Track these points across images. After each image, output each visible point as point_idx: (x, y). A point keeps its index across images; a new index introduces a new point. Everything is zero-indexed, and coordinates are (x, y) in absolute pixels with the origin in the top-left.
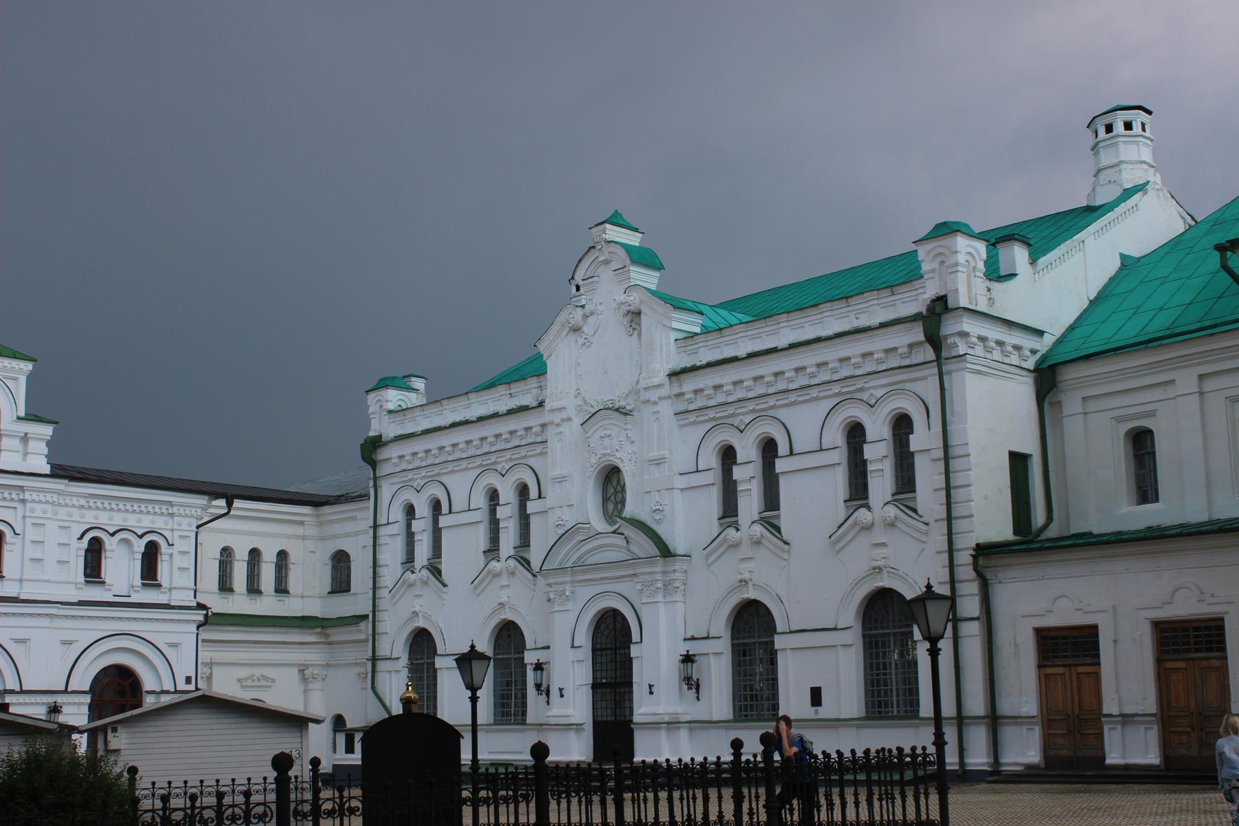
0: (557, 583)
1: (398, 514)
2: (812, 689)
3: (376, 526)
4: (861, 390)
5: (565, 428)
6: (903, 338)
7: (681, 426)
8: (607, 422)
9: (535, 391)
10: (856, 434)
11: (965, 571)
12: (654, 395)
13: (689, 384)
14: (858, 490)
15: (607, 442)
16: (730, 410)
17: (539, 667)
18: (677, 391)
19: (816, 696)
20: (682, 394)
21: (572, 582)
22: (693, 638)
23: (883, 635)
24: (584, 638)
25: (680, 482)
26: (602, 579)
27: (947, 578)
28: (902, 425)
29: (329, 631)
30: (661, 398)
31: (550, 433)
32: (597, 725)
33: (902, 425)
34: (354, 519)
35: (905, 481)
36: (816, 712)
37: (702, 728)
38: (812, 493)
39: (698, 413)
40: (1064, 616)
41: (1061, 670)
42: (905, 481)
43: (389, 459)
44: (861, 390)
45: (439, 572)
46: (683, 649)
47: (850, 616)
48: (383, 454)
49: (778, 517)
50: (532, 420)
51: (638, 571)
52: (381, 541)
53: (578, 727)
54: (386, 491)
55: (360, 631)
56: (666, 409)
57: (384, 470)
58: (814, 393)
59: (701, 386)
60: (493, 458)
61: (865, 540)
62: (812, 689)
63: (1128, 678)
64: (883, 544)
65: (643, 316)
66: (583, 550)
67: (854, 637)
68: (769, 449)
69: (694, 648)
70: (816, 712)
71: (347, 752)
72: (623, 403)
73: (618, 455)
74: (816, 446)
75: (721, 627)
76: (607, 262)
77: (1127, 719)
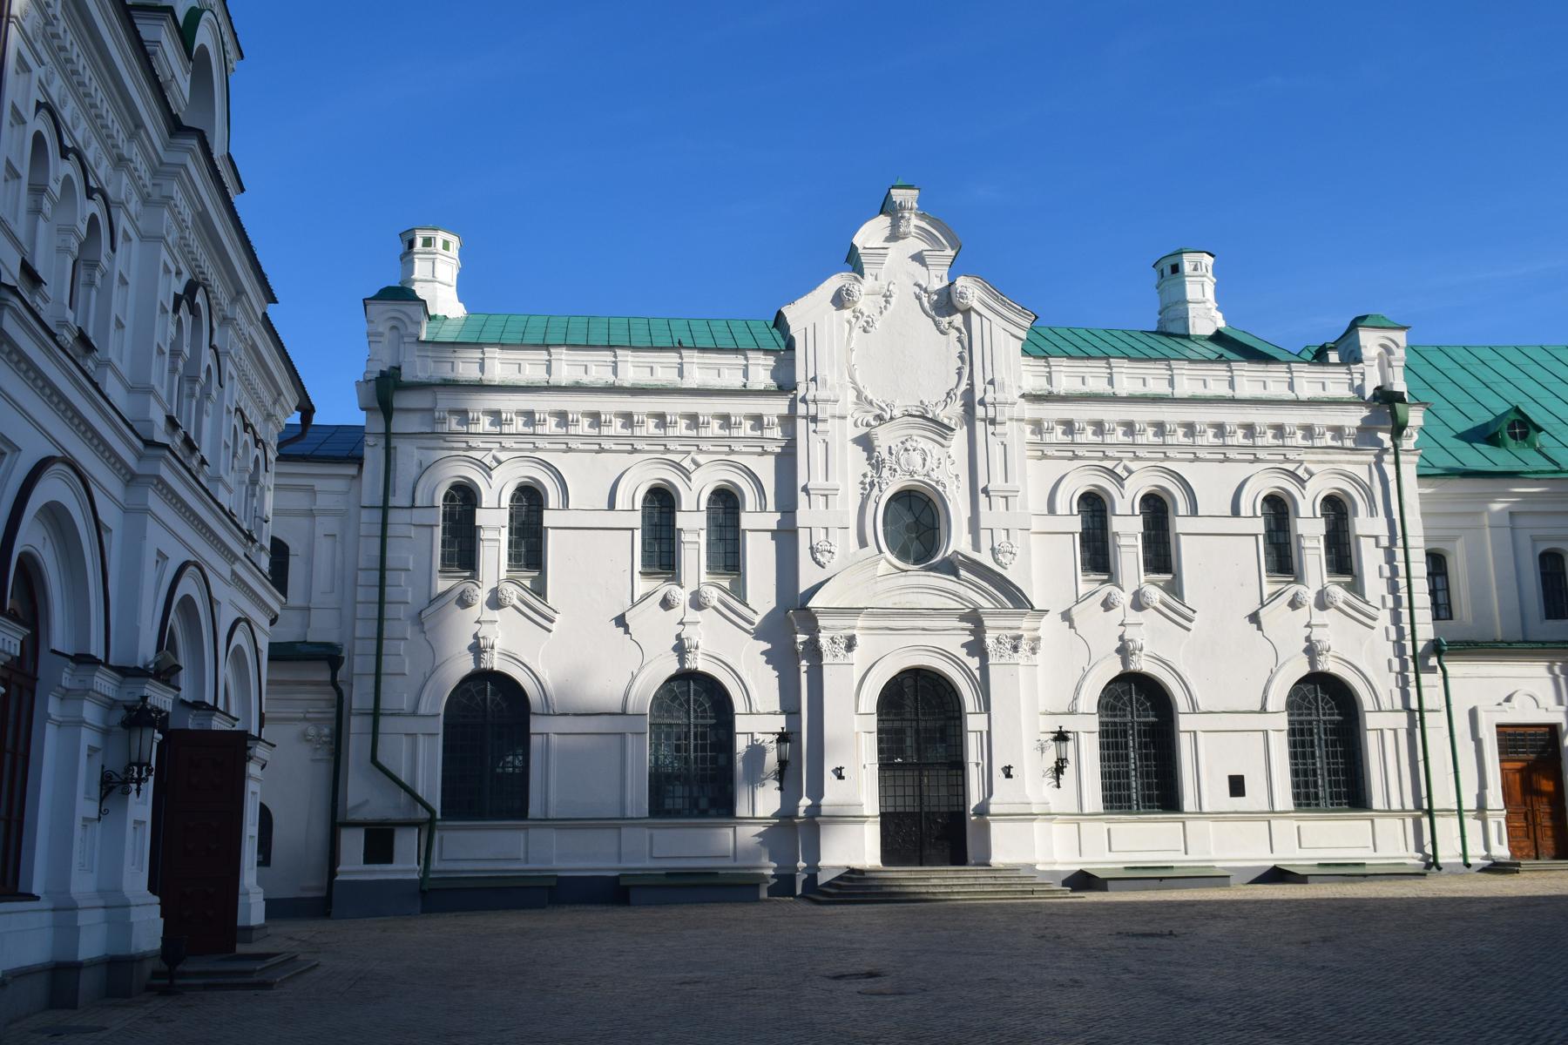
2: (1231, 777)
10: (1278, 509)
19: (1237, 786)
25: (1036, 524)
28: (1336, 509)
32: (882, 815)
47: (1278, 698)
48: (401, 400)
52: (391, 531)
57: (400, 424)
62: (1231, 777)
69: (1068, 724)
71: (369, 859)
73: (934, 475)
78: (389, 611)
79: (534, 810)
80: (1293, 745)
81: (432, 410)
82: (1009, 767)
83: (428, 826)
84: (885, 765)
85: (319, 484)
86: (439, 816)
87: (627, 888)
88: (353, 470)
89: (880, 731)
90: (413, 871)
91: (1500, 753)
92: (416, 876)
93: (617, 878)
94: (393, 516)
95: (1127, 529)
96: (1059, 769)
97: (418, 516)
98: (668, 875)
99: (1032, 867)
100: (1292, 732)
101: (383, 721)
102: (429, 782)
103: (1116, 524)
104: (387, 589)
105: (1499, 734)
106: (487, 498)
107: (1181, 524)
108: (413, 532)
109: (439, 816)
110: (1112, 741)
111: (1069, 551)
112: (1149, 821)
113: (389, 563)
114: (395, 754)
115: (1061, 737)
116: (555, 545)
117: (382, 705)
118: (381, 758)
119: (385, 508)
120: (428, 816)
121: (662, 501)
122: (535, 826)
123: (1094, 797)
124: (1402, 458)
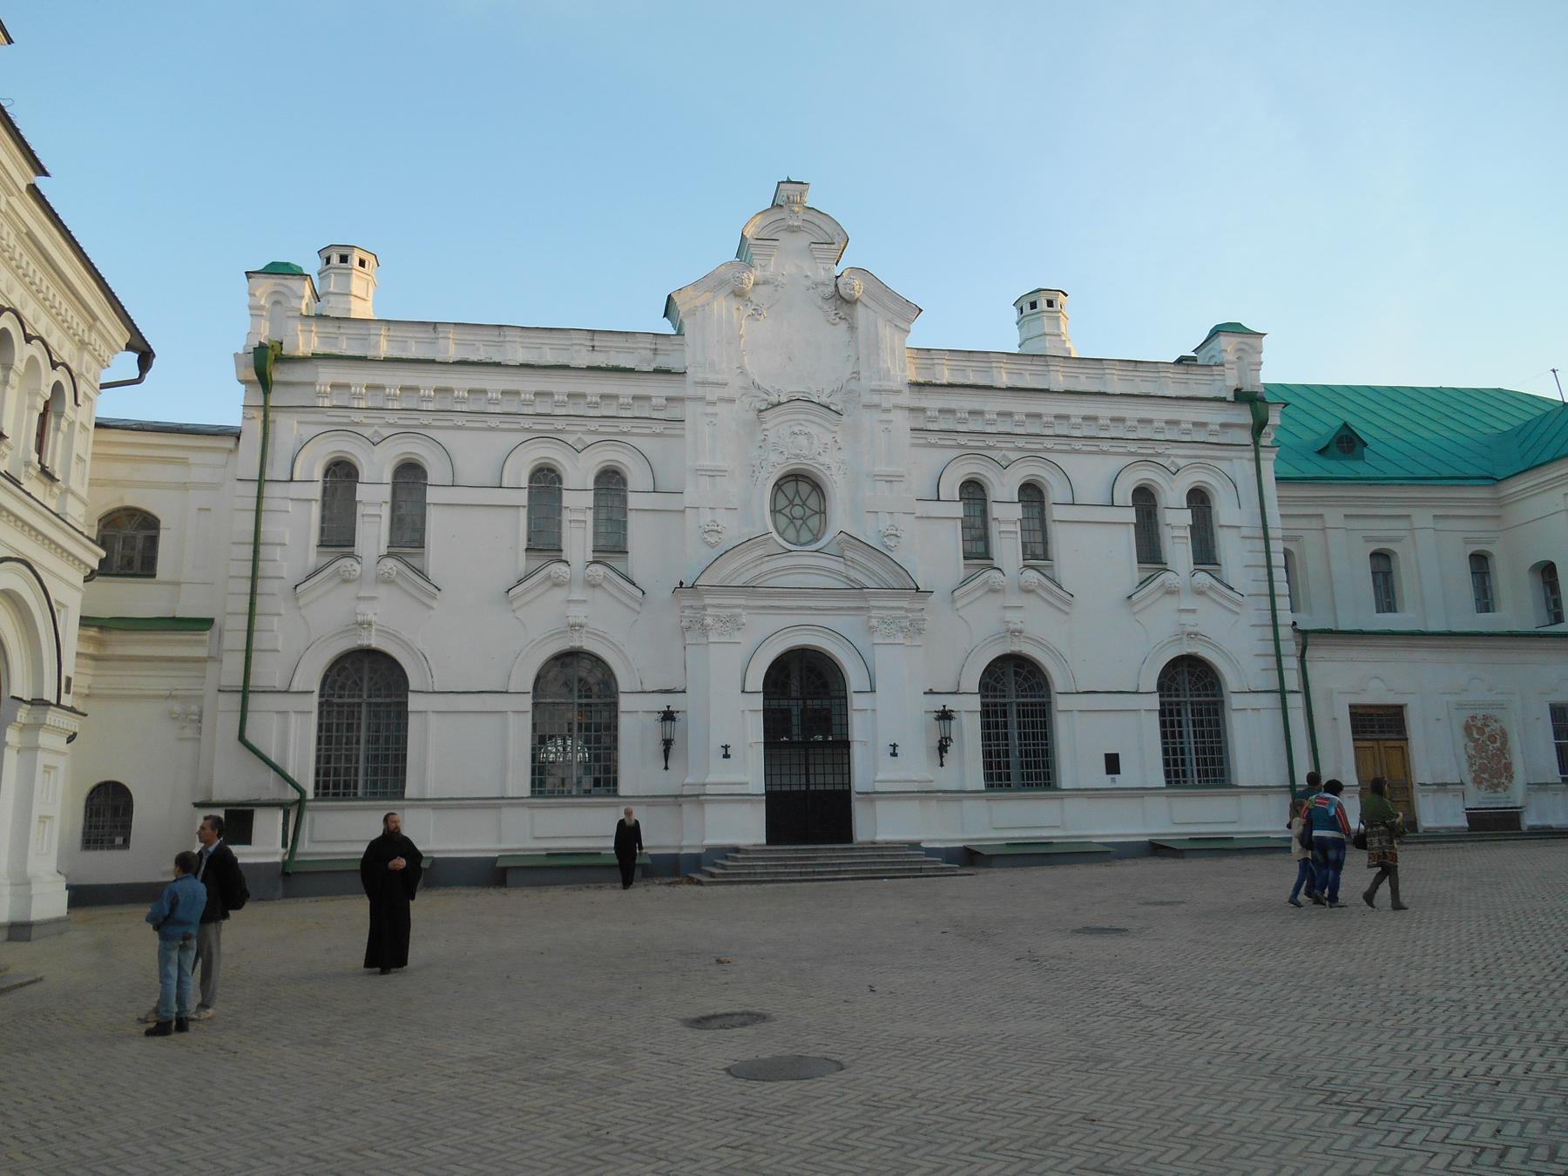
0: (719, 606)
1: (313, 466)
3: (261, 481)
4: (1158, 455)
5: (721, 409)
6: (1214, 416)
7: (914, 445)
8: (802, 416)
9: (649, 354)
10: (1145, 498)
11: (1290, 647)
12: (887, 401)
13: (933, 401)
14: (1150, 551)
15: (803, 440)
16: (991, 441)
17: (668, 716)
18: (916, 404)
19: (1112, 764)
20: (923, 410)
21: (746, 607)
22: (931, 692)
23: (1178, 704)
24: (756, 681)
26: (802, 608)
27: (1272, 651)
28: (1199, 499)
29: (107, 636)
30: (896, 407)
31: (690, 411)
32: (769, 794)
33: (1199, 499)
34: (184, 462)
35: (1205, 553)
36: (1113, 780)
37: (952, 800)
38: (1095, 549)
39: (942, 435)
40: (1377, 694)
41: (1370, 744)
42: (1205, 553)
43: (313, 384)
44: (1158, 455)
45: (421, 573)
46: (938, 703)
49: (1051, 567)
50: (659, 389)
51: (873, 603)
53: (745, 797)
54: (288, 429)
55: (201, 643)
56: (902, 421)
58: (1105, 446)
59: (953, 406)
60: (560, 424)
61: (1170, 603)
63: (1434, 753)
64: (1194, 611)
65: (859, 306)
66: (765, 567)
67: (1154, 702)
68: (1032, 493)
69: (951, 703)
70: (1113, 780)
72: (824, 400)
73: (821, 459)
74: (1106, 499)
75: (972, 681)
76: (792, 230)
77: (1442, 787)
78: (262, 586)
79: (410, 791)
80: (1163, 724)
81: (313, 384)
82: (894, 746)
83: (295, 809)
84: (771, 743)
85: (193, 457)
86: (310, 795)
87: (505, 870)
88: (229, 443)
89: (765, 711)
90: (275, 853)
91: (1354, 732)
92: (278, 859)
93: (495, 860)
94: (269, 490)
95: (1006, 515)
96: (943, 748)
97: (294, 490)
98: (548, 855)
99: (915, 845)
100: (1162, 713)
101: (255, 701)
102: (302, 762)
103: (996, 511)
104: (261, 564)
105: (1351, 714)
106: (365, 474)
107: (1055, 513)
108: (290, 506)
109: (310, 795)
110: (992, 718)
111: (951, 540)
112: (1035, 798)
113: (263, 538)
114: (264, 732)
115: (945, 716)
116: (436, 523)
117: (251, 683)
118: (250, 736)
119: (261, 481)
120: (296, 796)
121: (546, 480)
122: (411, 806)
123: (975, 776)
124: (1262, 455)
